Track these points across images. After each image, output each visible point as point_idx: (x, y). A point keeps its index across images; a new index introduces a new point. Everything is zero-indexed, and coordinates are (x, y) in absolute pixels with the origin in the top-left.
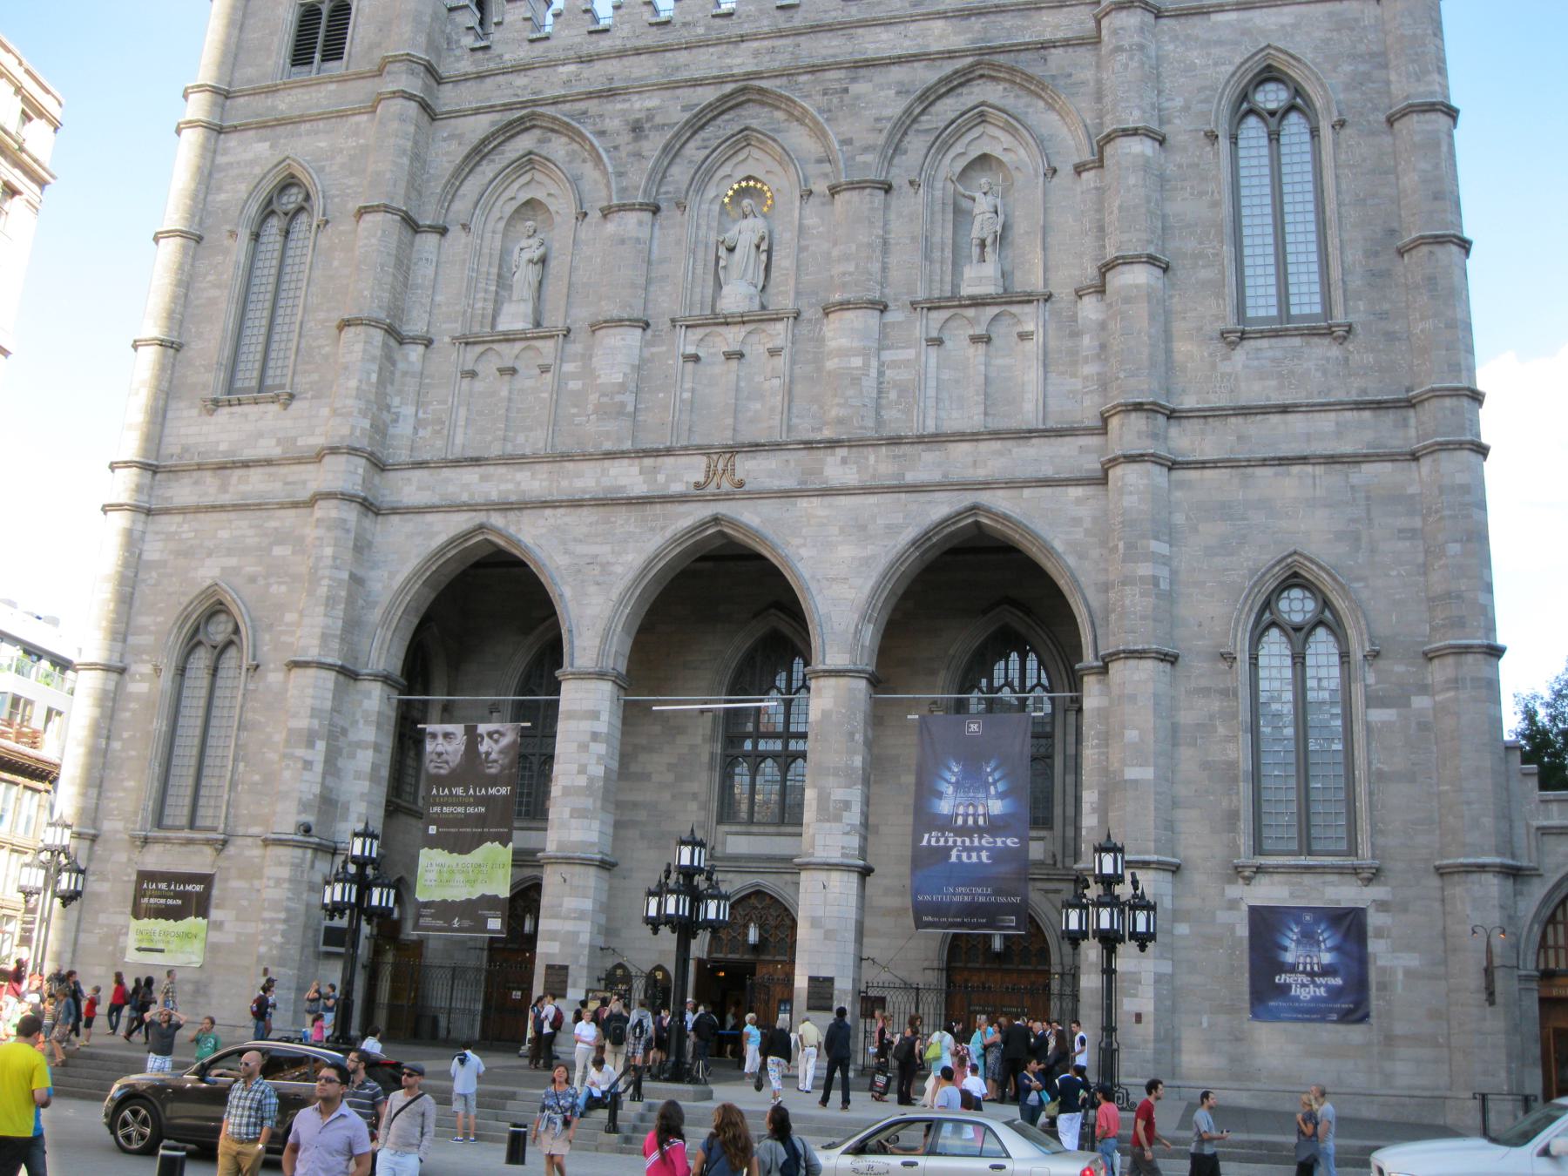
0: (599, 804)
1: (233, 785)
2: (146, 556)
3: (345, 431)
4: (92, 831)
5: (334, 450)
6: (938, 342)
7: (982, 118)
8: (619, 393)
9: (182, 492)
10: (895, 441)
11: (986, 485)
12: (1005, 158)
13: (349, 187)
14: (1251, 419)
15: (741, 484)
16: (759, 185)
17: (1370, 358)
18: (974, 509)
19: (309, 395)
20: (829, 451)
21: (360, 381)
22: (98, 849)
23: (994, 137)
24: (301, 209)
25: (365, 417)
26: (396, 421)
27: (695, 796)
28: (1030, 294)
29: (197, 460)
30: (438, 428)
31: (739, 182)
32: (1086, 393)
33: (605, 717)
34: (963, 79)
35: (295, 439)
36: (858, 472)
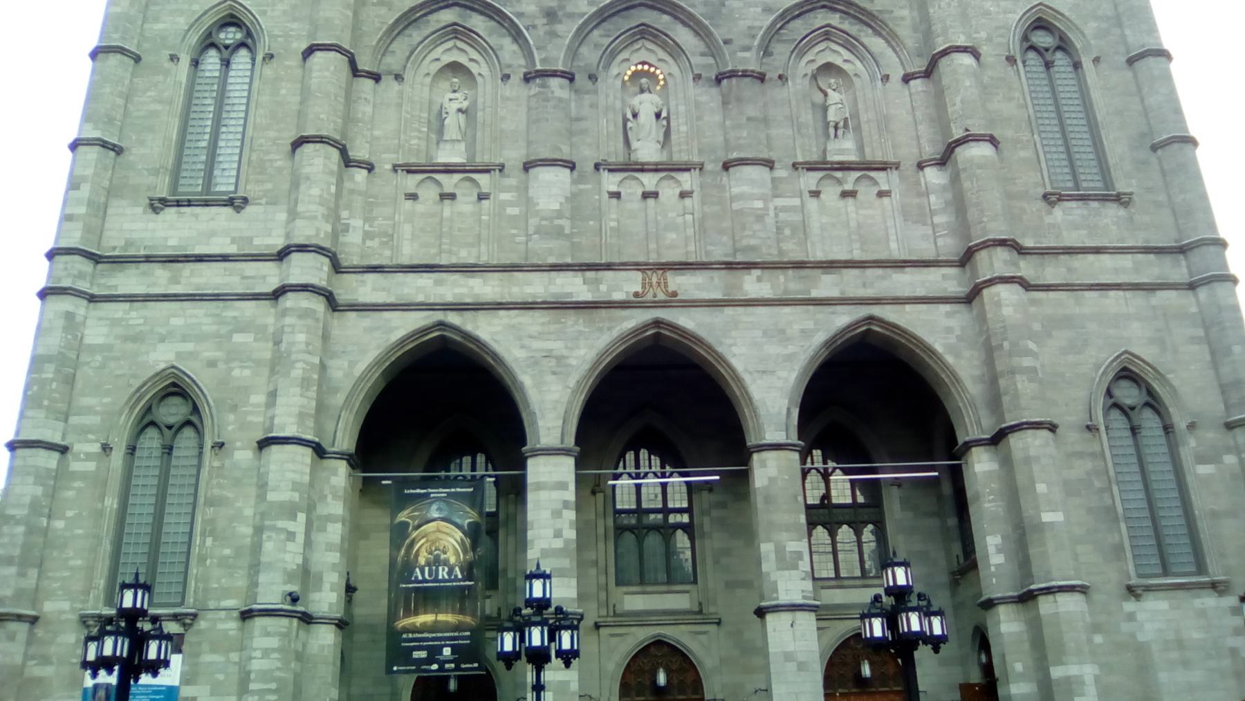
0: (575, 564)
1: (202, 560)
2: (87, 341)
3: (310, 232)
4: (33, 613)
5: (302, 248)
6: (816, 194)
7: (827, 36)
8: (557, 218)
9: (129, 281)
10: (799, 265)
11: (877, 301)
12: (845, 66)
13: (292, 30)
14: (1075, 257)
15: (675, 294)
16: (652, 70)
18: (871, 319)
19: (264, 201)
20: (746, 271)
21: (323, 190)
22: (39, 632)
23: (834, 51)
24: (242, 45)
25: (327, 222)
26: (346, 229)
27: (596, 563)
28: (885, 163)
29: (142, 252)
30: (385, 240)
31: (636, 65)
32: (941, 236)
33: (572, 487)
34: (810, 7)
35: (250, 239)
36: (772, 288)
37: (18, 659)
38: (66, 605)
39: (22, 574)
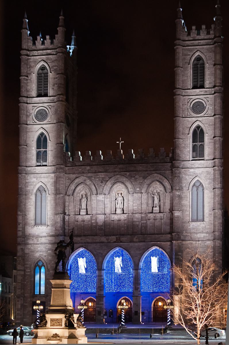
3: (59, 233)
17: (208, 227)
35: (49, 233)
37: (23, 303)
38: (28, 295)
39: (21, 291)
